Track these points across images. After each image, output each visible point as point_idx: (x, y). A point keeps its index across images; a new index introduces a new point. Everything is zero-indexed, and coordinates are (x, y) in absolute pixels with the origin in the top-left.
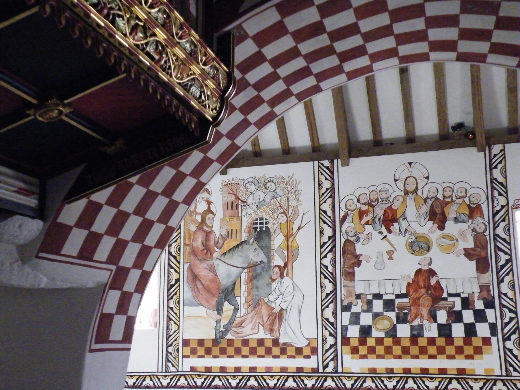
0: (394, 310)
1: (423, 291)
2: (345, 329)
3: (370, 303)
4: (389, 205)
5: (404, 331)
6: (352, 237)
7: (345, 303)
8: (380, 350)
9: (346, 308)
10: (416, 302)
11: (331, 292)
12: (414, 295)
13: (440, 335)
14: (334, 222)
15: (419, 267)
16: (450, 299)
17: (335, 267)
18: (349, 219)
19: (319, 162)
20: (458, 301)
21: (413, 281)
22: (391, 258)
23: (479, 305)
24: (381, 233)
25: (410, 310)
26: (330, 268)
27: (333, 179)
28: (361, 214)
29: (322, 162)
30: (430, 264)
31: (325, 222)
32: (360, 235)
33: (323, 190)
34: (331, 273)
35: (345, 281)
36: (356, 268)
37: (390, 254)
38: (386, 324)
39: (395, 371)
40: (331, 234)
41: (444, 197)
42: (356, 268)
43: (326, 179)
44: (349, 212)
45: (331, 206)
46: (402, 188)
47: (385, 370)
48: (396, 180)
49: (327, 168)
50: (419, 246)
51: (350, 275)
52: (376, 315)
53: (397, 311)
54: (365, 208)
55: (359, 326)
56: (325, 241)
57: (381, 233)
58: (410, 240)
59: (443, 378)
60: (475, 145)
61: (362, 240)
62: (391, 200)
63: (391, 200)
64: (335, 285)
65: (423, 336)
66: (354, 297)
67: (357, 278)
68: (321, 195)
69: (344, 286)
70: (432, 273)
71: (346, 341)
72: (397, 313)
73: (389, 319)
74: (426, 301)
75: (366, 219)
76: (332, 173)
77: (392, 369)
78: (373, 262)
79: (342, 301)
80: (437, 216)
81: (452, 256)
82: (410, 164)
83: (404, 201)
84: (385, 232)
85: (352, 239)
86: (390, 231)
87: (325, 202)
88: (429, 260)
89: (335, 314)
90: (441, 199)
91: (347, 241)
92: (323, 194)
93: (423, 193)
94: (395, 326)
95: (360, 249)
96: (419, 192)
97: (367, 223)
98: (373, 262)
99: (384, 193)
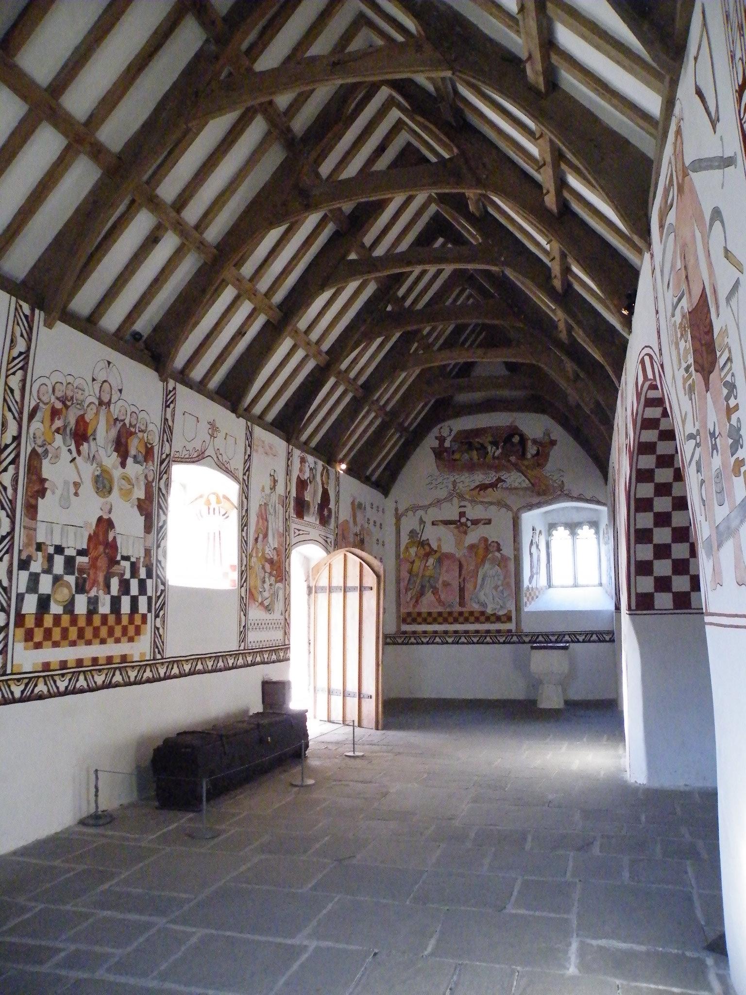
0: (73, 573)
1: (101, 548)
2: (20, 598)
3: (50, 559)
4: (82, 413)
5: (81, 606)
6: (40, 446)
7: (24, 557)
8: (57, 634)
9: (24, 565)
10: (93, 564)
11: (8, 534)
12: (94, 554)
13: (112, 612)
14: (21, 413)
15: (100, 513)
16: (123, 563)
17: (15, 490)
18: (39, 415)
19: (17, 302)
20: (126, 564)
21: (95, 533)
22: (76, 494)
23: (143, 573)
24: (70, 451)
25: (88, 575)
26: (10, 491)
27: (30, 339)
28: (55, 413)
29: (22, 303)
30: (110, 512)
31: (10, 410)
32: (49, 447)
33: (15, 353)
34: (10, 501)
35: (27, 519)
36: (40, 499)
37: (77, 485)
38: (63, 594)
39: (69, 665)
40: (15, 434)
41: (130, 424)
42: (40, 499)
43: (22, 335)
44: (41, 405)
45: (20, 385)
46: (98, 395)
47: (41, 666)
48: (94, 380)
49: (26, 316)
50: (103, 484)
51: (32, 510)
52: (57, 579)
53: (76, 574)
54: (59, 405)
55: (36, 596)
56: (8, 443)
57: (70, 451)
58: (97, 473)
59: (108, 669)
60: (157, 370)
61: (50, 455)
62: (86, 406)
63: (86, 406)
64: (13, 523)
65: (97, 613)
66: (35, 546)
67: (40, 516)
68: (11, 358)
69: (25, 527)
70: (110, 524)
71: (20, 619)
72: (77, 579)
73: (68, 585)
74: (102, 563)
75: (58, 423)
76: (31, 328)
77: (65, 662)
78: (58, 492)
79: (20, 551)
80: (121, 447)
81: (128, 505)
82: (109, 363)
83: (97, 414)
84: (75, 454)
85: (40, 450)
86: (79, 453)
87: (14, 374)
88: (109, 507)
89: (10, 572)
90: (128, 425)
91: (34, 451)
92: (14, 359)
93: (115, 410)
94: (74, 596)
95: (47, 470)
96: (112, 406)
97: (58, 431)
98: (58, 492)
99: (80, 392)
